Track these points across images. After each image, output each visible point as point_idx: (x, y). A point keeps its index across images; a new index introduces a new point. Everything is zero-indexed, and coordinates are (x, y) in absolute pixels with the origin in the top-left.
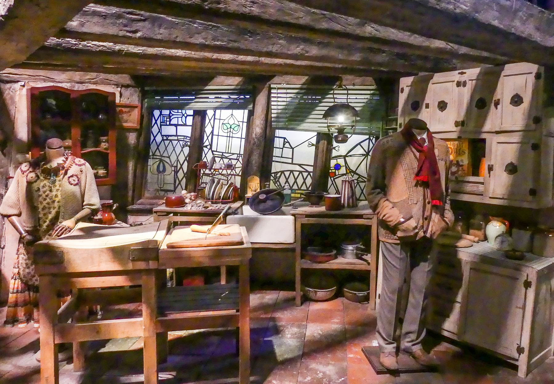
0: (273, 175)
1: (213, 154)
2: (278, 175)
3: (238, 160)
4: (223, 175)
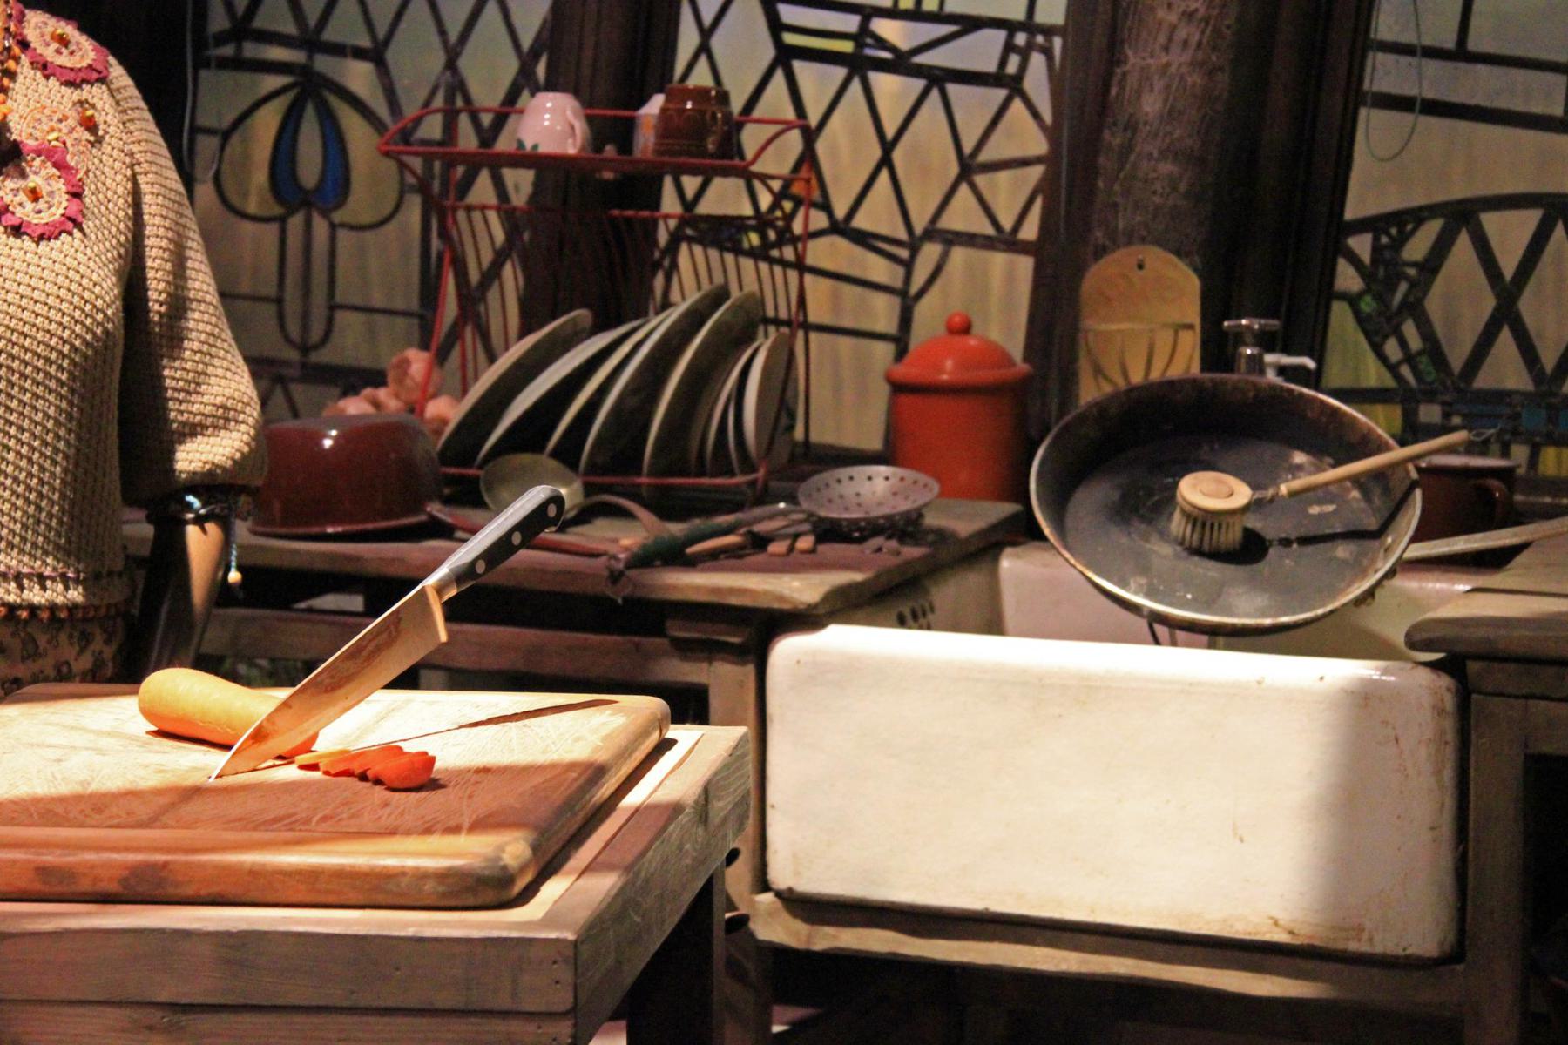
0: (1361, 245)
1: (777, 27)
2: (1418, 247)
3: (1014, 86)
4: (864, 239)
